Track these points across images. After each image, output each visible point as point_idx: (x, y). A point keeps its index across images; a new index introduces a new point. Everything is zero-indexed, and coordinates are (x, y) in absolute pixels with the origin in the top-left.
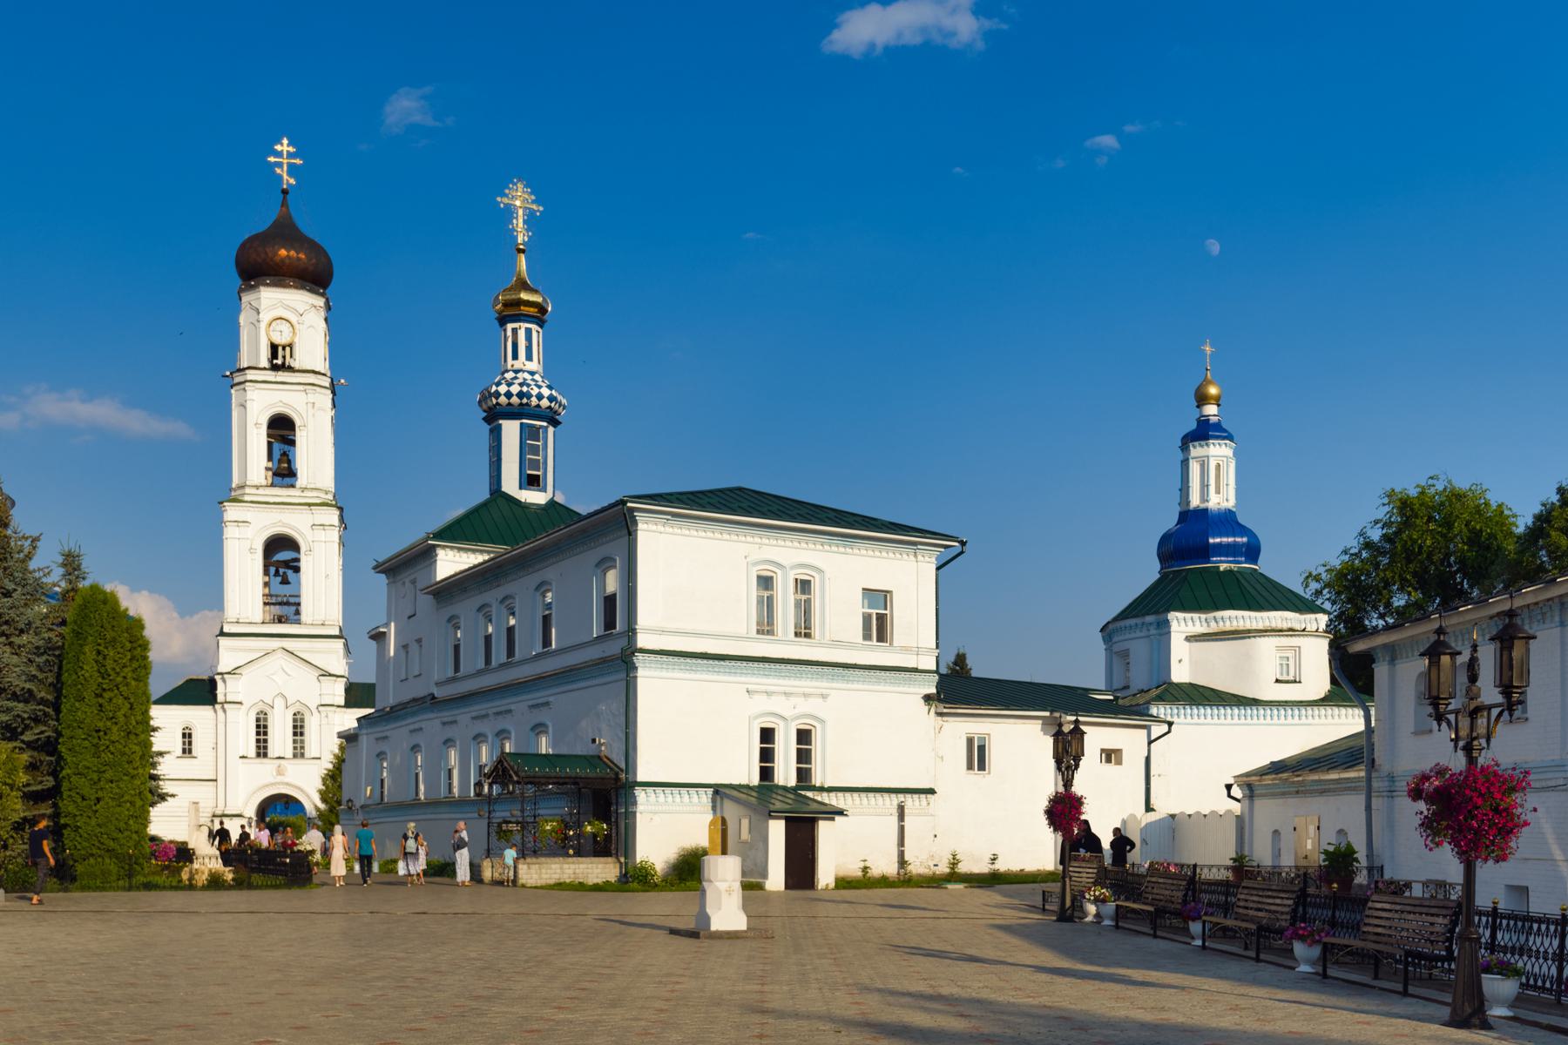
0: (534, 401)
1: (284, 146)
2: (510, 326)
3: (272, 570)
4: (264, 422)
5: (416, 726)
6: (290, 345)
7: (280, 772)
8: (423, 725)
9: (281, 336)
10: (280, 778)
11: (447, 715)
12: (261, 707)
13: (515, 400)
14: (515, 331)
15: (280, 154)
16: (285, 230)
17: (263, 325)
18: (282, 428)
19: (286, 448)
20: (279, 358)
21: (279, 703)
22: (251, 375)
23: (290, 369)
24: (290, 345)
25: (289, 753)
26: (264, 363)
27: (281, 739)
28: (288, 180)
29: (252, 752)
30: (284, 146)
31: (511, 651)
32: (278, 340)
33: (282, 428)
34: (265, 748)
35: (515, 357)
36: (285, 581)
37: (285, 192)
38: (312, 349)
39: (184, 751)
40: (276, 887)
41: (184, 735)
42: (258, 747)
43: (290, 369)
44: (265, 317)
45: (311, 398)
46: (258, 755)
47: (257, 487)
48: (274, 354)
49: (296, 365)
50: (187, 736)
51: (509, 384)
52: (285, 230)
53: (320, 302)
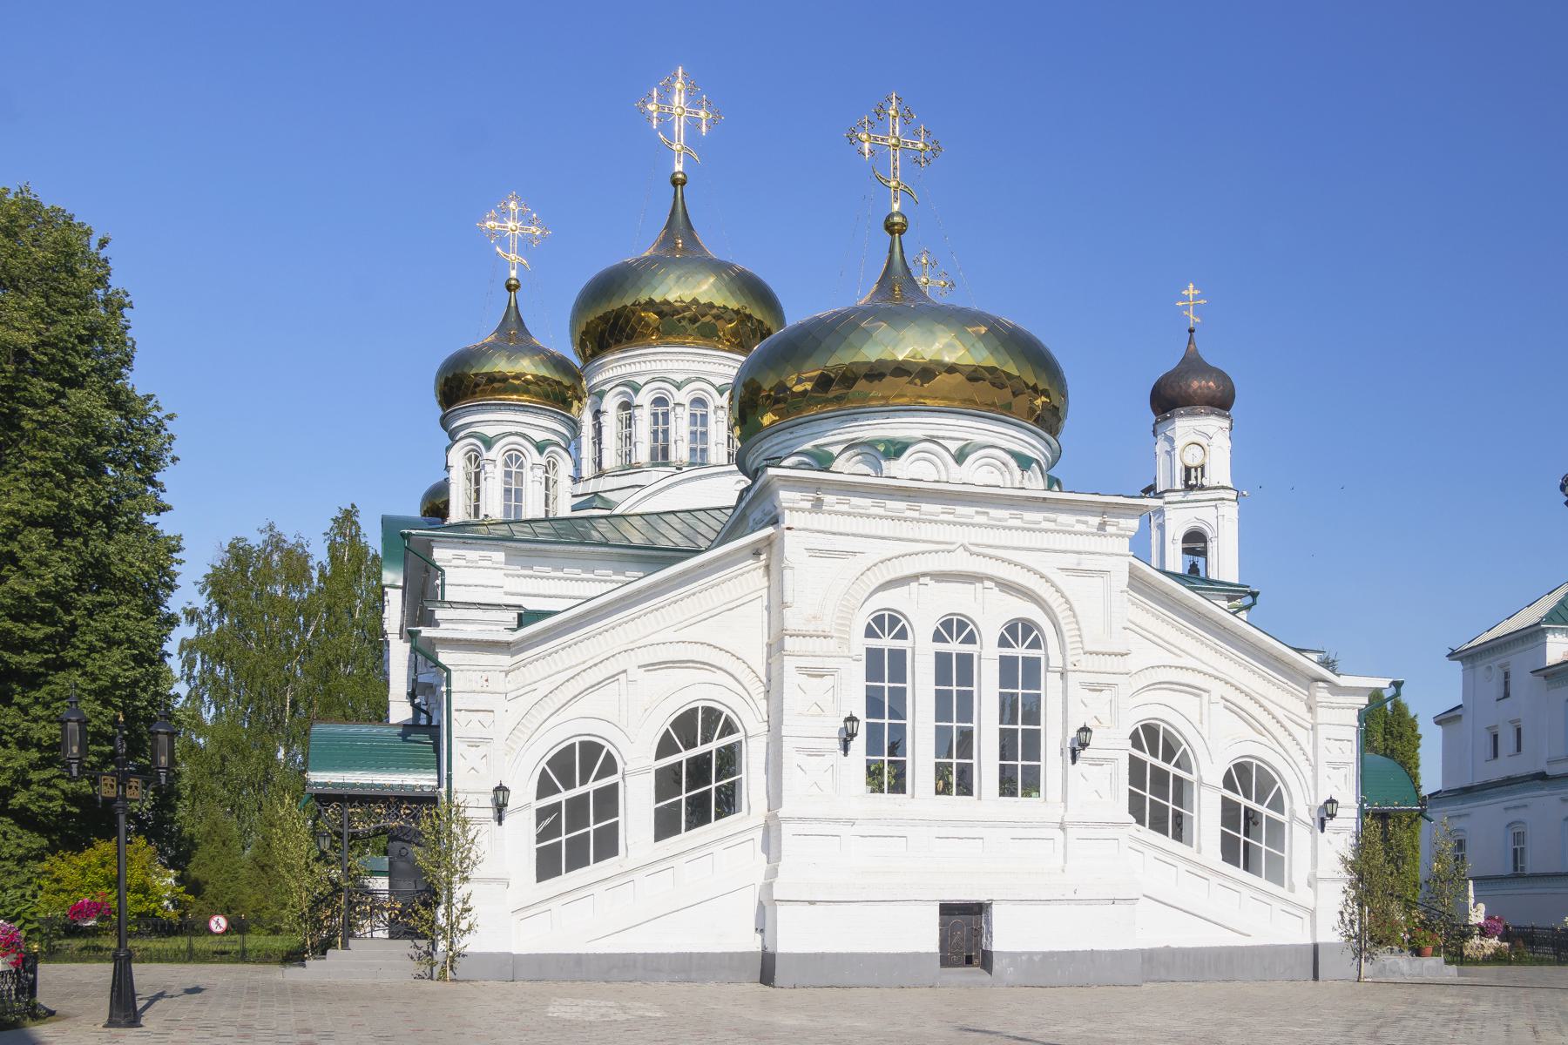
1: (1191, 291)
4: (1180, 537)
9: (1193, 458)
15: (1186, 298)
16: (1192, 364)
17: (1177, 452)
18: (1195, 542)
20: (1192, 480)
22: (1169, 497)
24: (1203, 467)
26: (1179, 485)
28: (1193, 320)
30: (1191, 291)
32: (1190, 463)
33: (1195, 542)
37: (1191, 331)
38: (1219, 470)
40: (1540, 962)
43: (1202, 488)
44: (1179, 444)
48: (1188, 477)
49: (1206, 482)
52: (1192, 364)
53: (1226, 423)
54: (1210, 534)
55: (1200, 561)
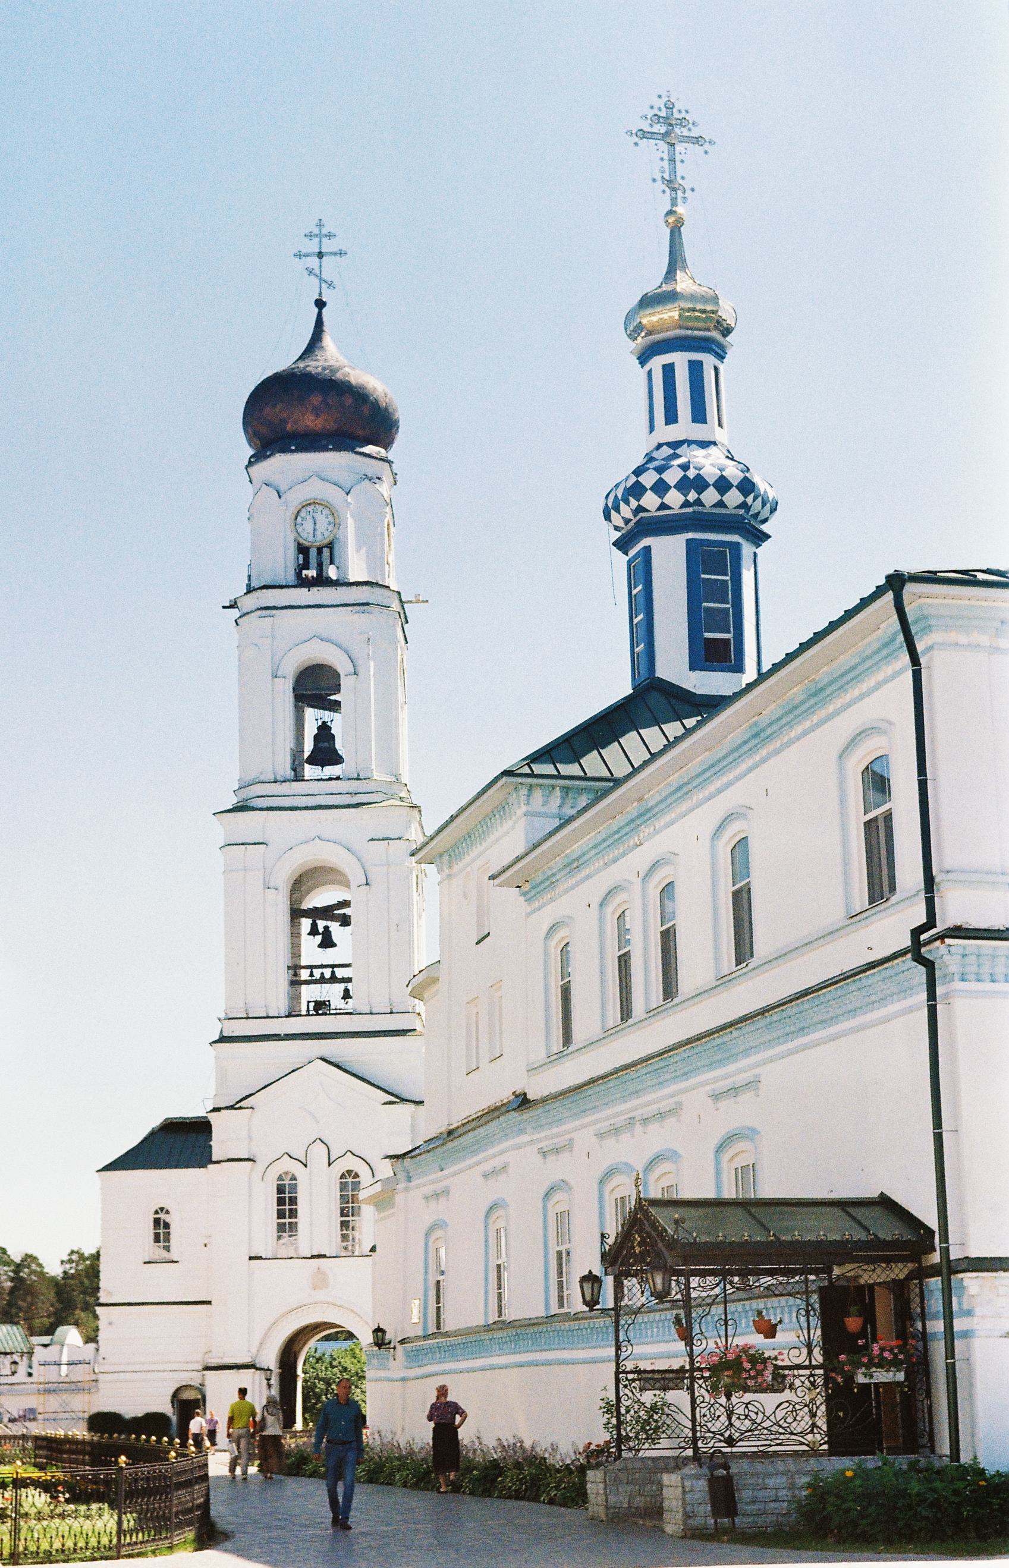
0: (710, 496)
2: (657, 362)
3: (306, 923)
5: (497, 1162)
8: (510, 1157)
11: (548, 1136)
13: (674, 498)
14: (669, 370)
19: (326, 715)
21: (319, 1153)
31: (669, 989)
32: (308, 537)
35: (671, 418)
36: (327, 942)
49: (332, 573)
51: (660, 470)
55: (338, 723)
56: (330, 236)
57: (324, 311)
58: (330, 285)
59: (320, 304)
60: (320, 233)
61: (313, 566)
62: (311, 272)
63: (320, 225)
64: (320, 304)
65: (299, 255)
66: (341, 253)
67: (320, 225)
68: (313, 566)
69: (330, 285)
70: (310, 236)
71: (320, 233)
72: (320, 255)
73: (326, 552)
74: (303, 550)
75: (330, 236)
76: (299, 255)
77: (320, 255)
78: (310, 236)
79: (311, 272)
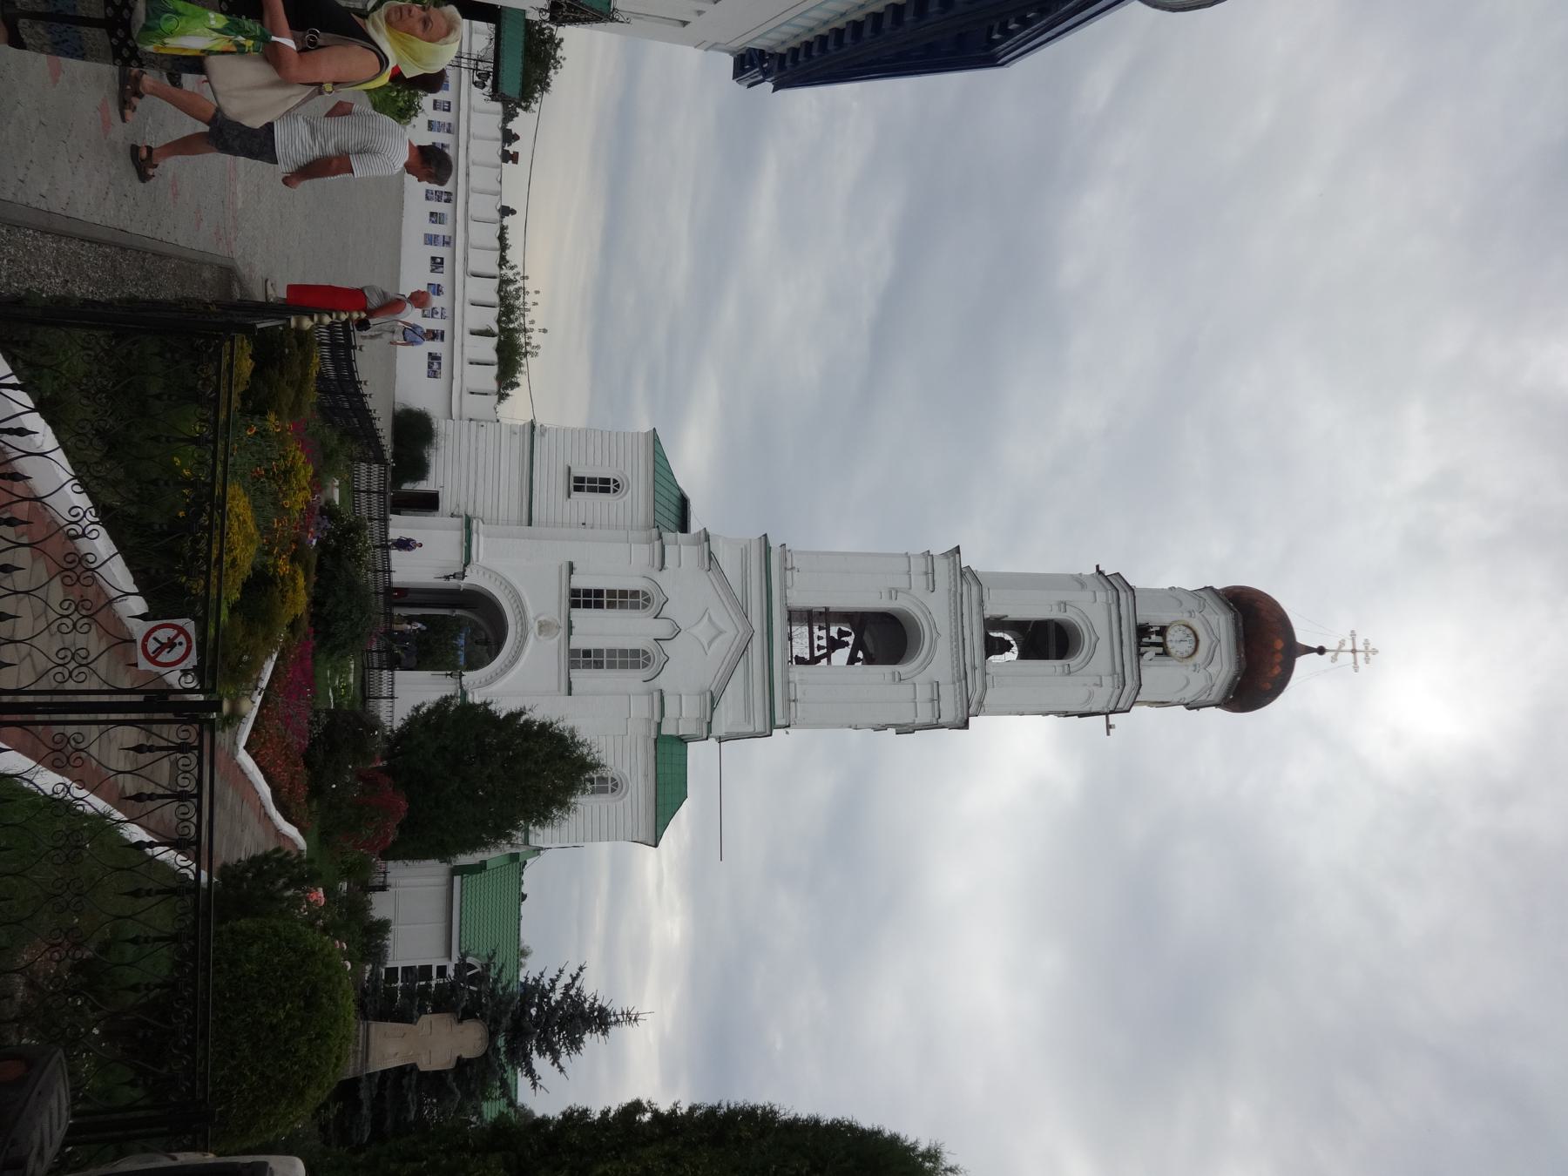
4: (1070, 616)
6: (1166, 653)
7: (544, 627)
10: (534, 627)
12: (657, 600)
21: (661, 628)
23: (1140, 655)
24: (1166, 653)
25: (578, 643)
27: (596, 629)
29: (580, 582)
32: (1173, 636)
34: (587, 605)
39: (580, 480)
41: (606, 481)
42: (587, 593)
45: (1107, 681)
46: (574, 593)
47: (981, 602)
50: (604, 486)
54: (1074, 662)
55: (1012, 655)
56: (1367, 660)
57: (1315, 655)
58: (1334, 659)
59: (1321, 651)
60: (1370, 652)
61: (1149, 638)
62: (1342, 643)
63: (1375, 652)
64: (1321, 651)
65: (1353, 634)
66: (1356, 668)
67: (1375, 652)
68: (1149, 638)
69: (1334, 659)
70: (1366, 643)
71: (1370, 652)
72: (1354, 651)
73: (1160, 650)
74: (1162, 631)
75: (1367, 660)
76: (1353, 634)
77: (1354, 651)
78: (1366, 643)
79: (1342, 643)
